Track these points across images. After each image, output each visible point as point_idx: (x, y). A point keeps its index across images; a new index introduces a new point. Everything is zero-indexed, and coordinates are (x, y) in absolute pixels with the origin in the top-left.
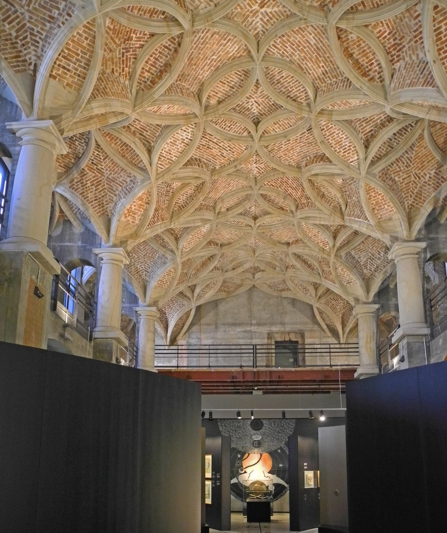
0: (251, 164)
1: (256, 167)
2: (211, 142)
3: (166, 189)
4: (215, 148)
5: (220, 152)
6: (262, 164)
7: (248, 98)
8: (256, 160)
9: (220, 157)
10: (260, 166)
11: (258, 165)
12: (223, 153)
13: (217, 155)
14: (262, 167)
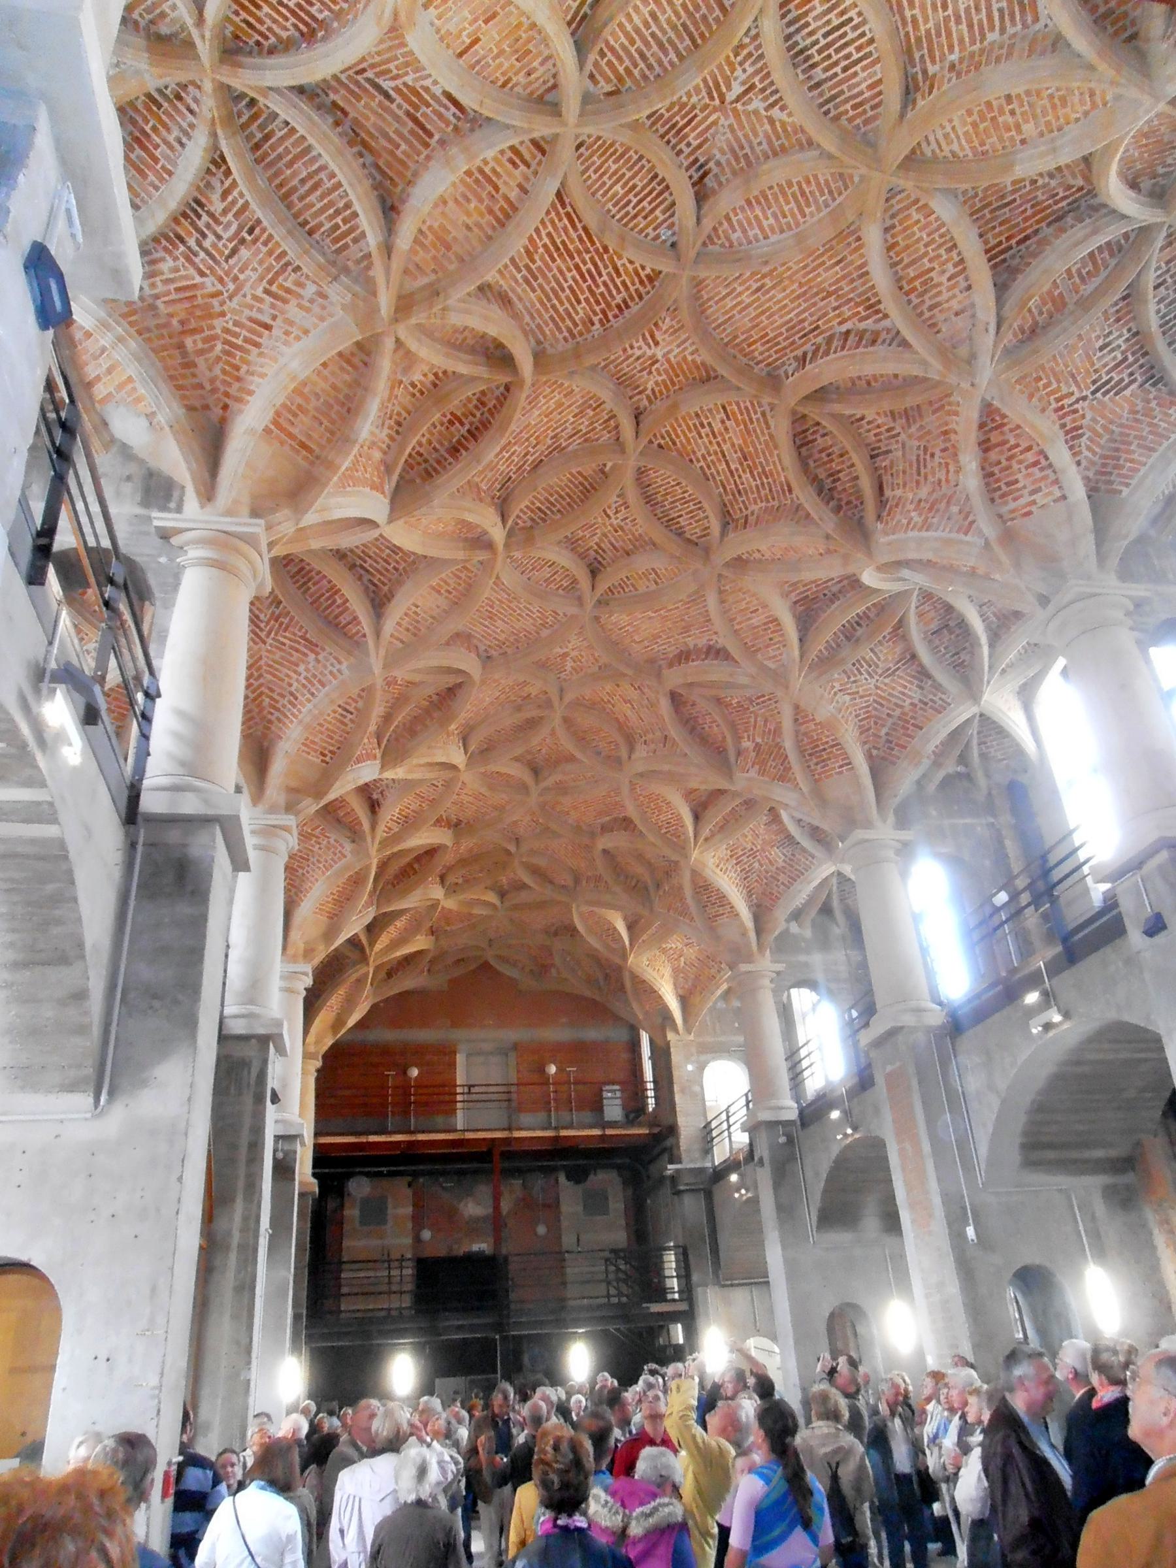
0: (668, 361)
1: (657, 344)
2: (733, 467)
3: (903, 436)
4: (733, 445)
5: (726, 429)
6: (638, 353)
7: (621, 528)
8: (650, 373)
9: (734, 414)
10: (645, 347)
11: (649, 353)
12: (723, 422)
13: (738, 425)
14: (641, 343)
